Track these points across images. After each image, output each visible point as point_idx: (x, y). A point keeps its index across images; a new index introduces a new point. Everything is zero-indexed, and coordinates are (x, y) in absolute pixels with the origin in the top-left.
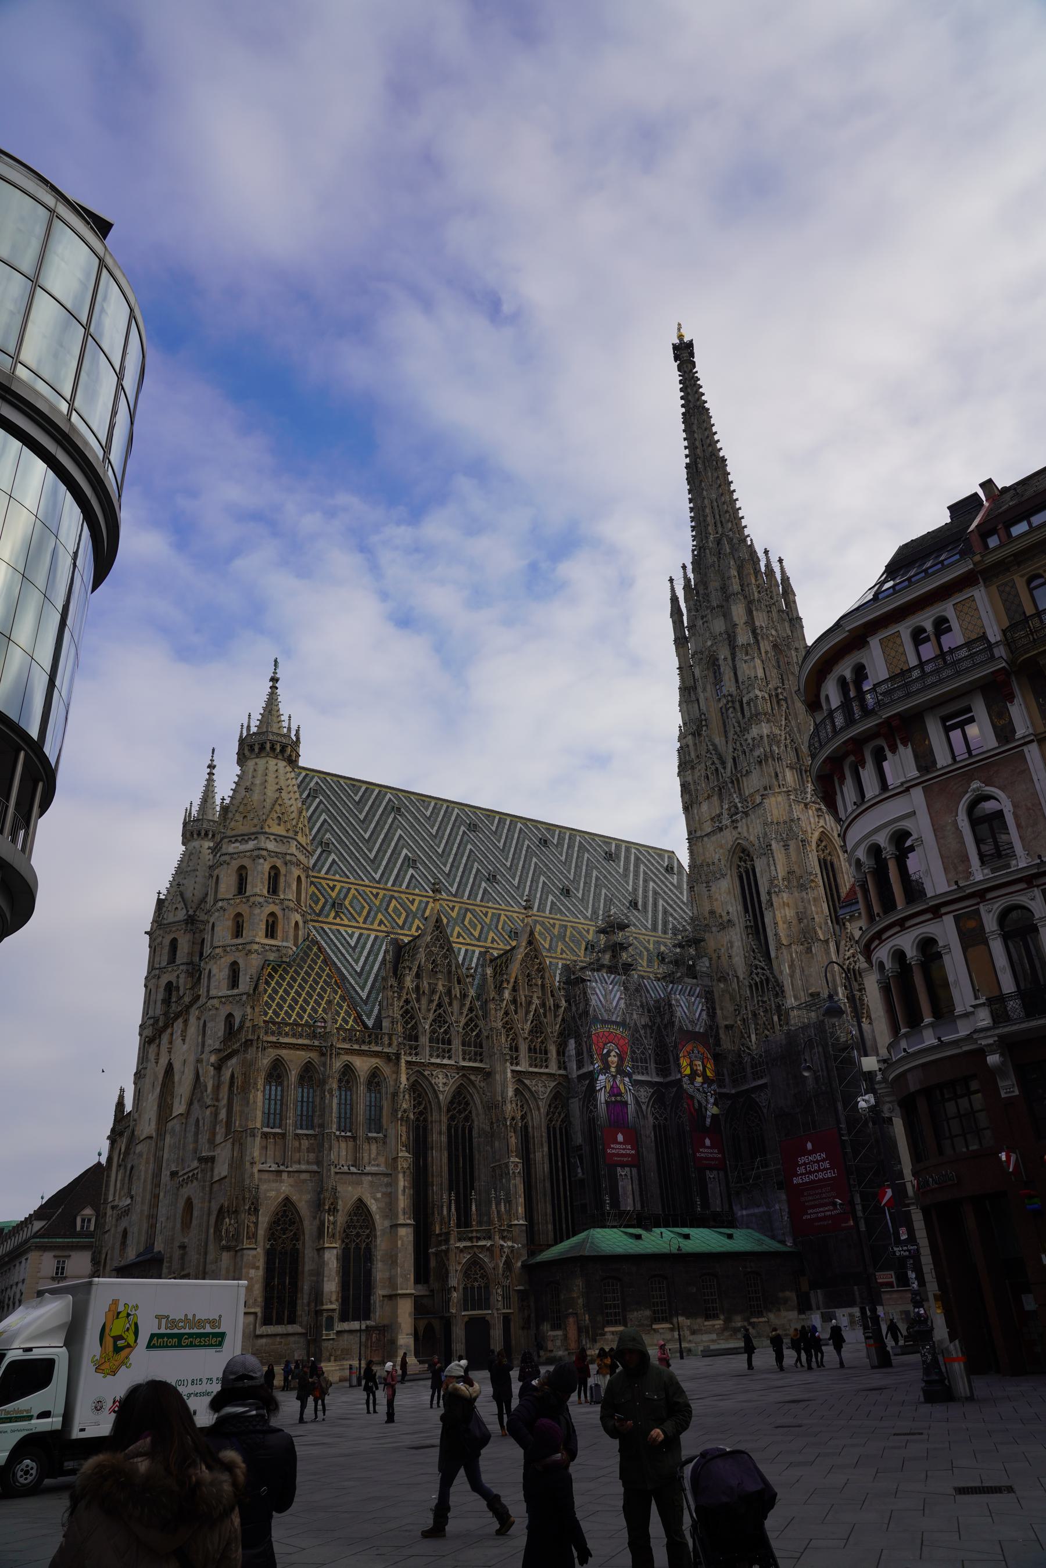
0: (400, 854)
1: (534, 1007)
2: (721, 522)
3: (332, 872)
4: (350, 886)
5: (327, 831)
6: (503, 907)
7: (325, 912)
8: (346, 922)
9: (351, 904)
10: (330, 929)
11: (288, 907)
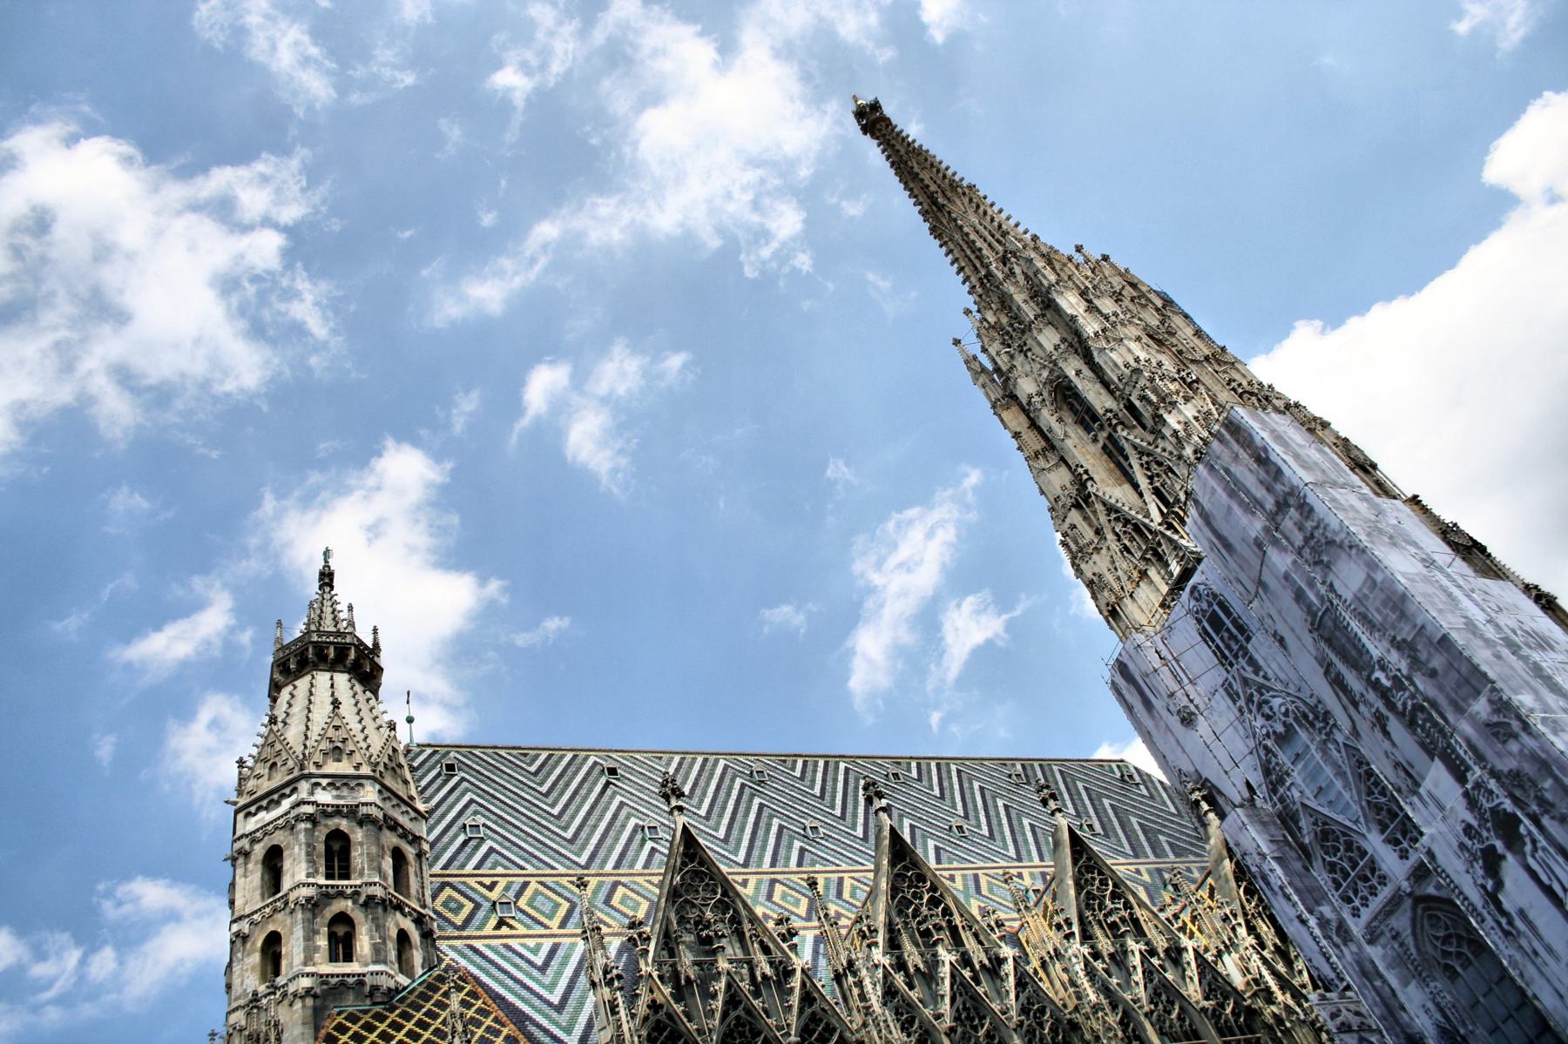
0: (623, 826)
1: (945, 971)
3: (488, 863)
4: (527, 879)
5: (476, 813)
6: (844, 867)
7: (476, 921)
8: (522, 930)
9: (530, 904)
10: (488, 946)
11: (371, 898)
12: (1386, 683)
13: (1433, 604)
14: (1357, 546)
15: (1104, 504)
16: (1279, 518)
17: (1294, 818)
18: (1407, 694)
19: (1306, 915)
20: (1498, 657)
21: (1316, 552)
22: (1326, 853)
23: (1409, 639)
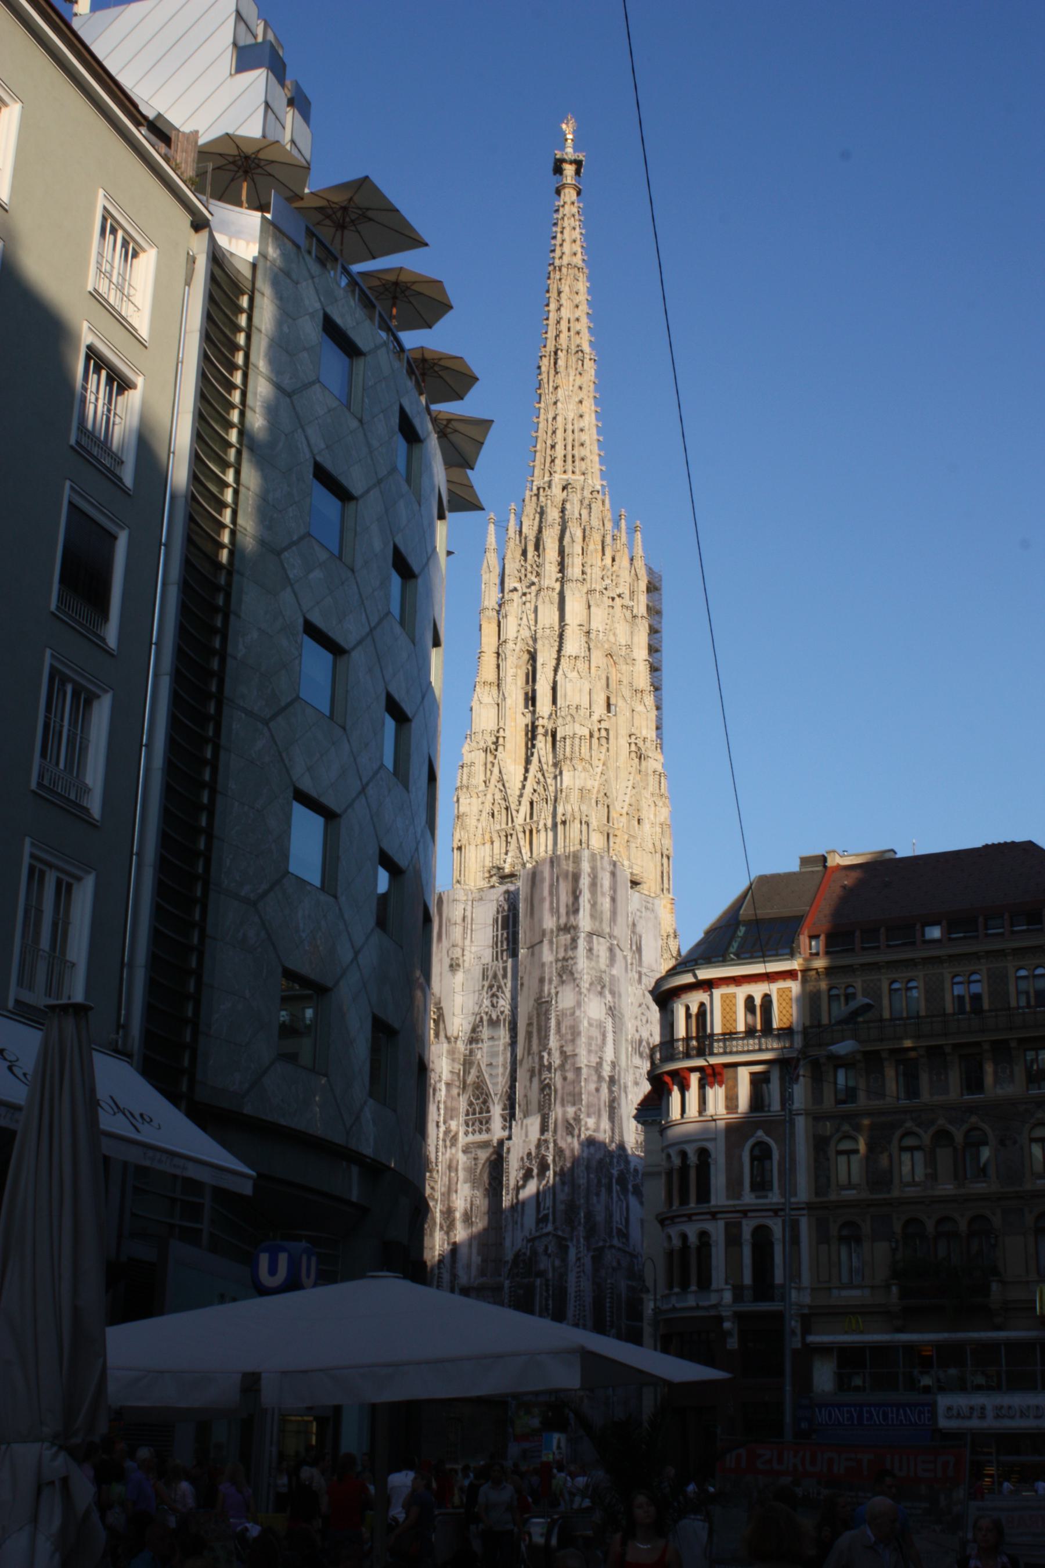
2: (573, 457)
12: (546, 1063)
13: (590, 1045)
14: (580, 988)
15: (500, 772)
16: (561, 933)
17: (471, 1063)
18: (549, 1076)
19: (441, 1124)
20: (597, 1090)
21: (563, 969)
22: (473, 1096)
23: (568, 1054)
